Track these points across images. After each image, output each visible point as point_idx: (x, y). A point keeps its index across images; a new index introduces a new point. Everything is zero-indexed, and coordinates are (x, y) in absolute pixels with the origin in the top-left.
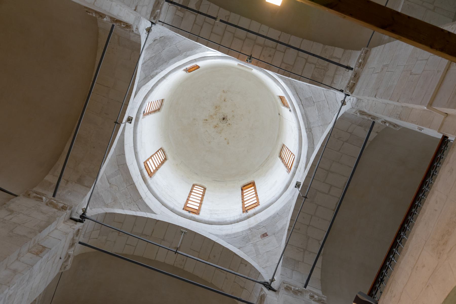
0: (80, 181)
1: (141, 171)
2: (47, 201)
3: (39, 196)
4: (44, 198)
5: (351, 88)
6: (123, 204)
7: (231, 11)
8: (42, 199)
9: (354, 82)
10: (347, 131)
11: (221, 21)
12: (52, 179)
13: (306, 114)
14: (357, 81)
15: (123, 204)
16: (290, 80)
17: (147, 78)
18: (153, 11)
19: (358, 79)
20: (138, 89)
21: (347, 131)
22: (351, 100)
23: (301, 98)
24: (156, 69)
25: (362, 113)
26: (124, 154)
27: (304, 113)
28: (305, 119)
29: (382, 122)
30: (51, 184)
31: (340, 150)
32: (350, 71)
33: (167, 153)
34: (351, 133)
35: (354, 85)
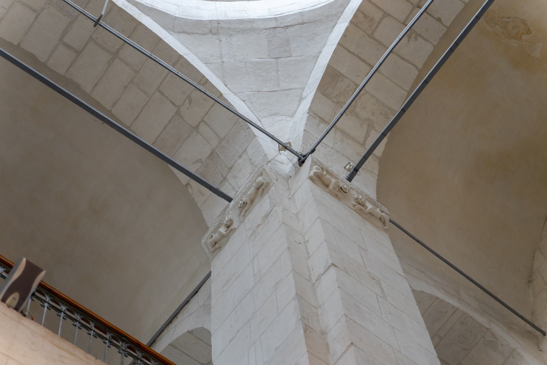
5: (320, 179)
9: (331, 187)
10: (203, 121)
13: (253, 30)
14: (330, 192)
16: (338, 15)
19: (336, 196)
21: (203, 121)
22: (286, 162)
23: (290, 29)
25: (261, 189)
27: (255, 25)
28: (242, 26)
29: (231, 221)
31: (160, 92)
32: (344, 175)
34: (197, 127)
35: (326, 185)
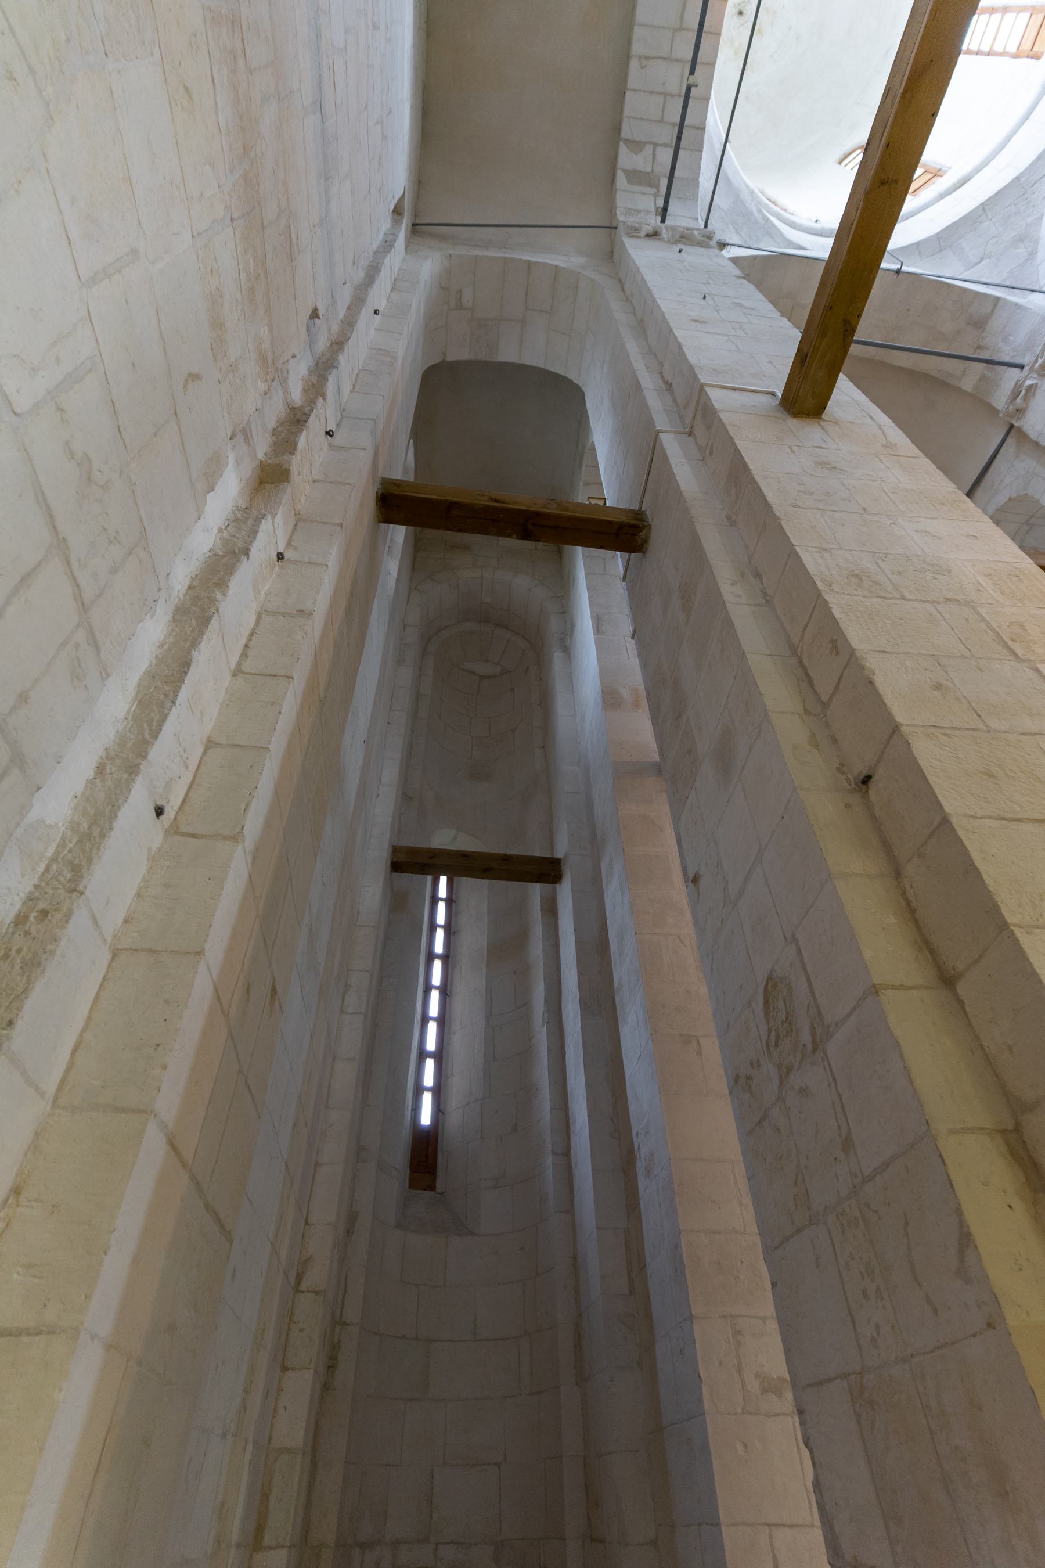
0: (980, 324)
1: (942, 196)
2: (1035, 376)
3: (1023, 392)
4: (1028, 383)
6: (1029, 220)
7: (628, 57)
8: (1031, 386)
11: (692, 72)
12: (969, 378)
15: (1029, 220)
17: (771, 231)
18: (700, 244)
20: (790, 244)
24: (752, 214)
26: (918, 244)
30: (983, 378)
33: (847, 149)
